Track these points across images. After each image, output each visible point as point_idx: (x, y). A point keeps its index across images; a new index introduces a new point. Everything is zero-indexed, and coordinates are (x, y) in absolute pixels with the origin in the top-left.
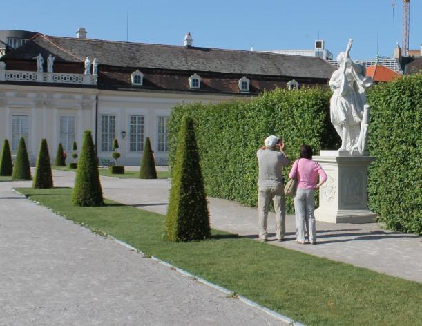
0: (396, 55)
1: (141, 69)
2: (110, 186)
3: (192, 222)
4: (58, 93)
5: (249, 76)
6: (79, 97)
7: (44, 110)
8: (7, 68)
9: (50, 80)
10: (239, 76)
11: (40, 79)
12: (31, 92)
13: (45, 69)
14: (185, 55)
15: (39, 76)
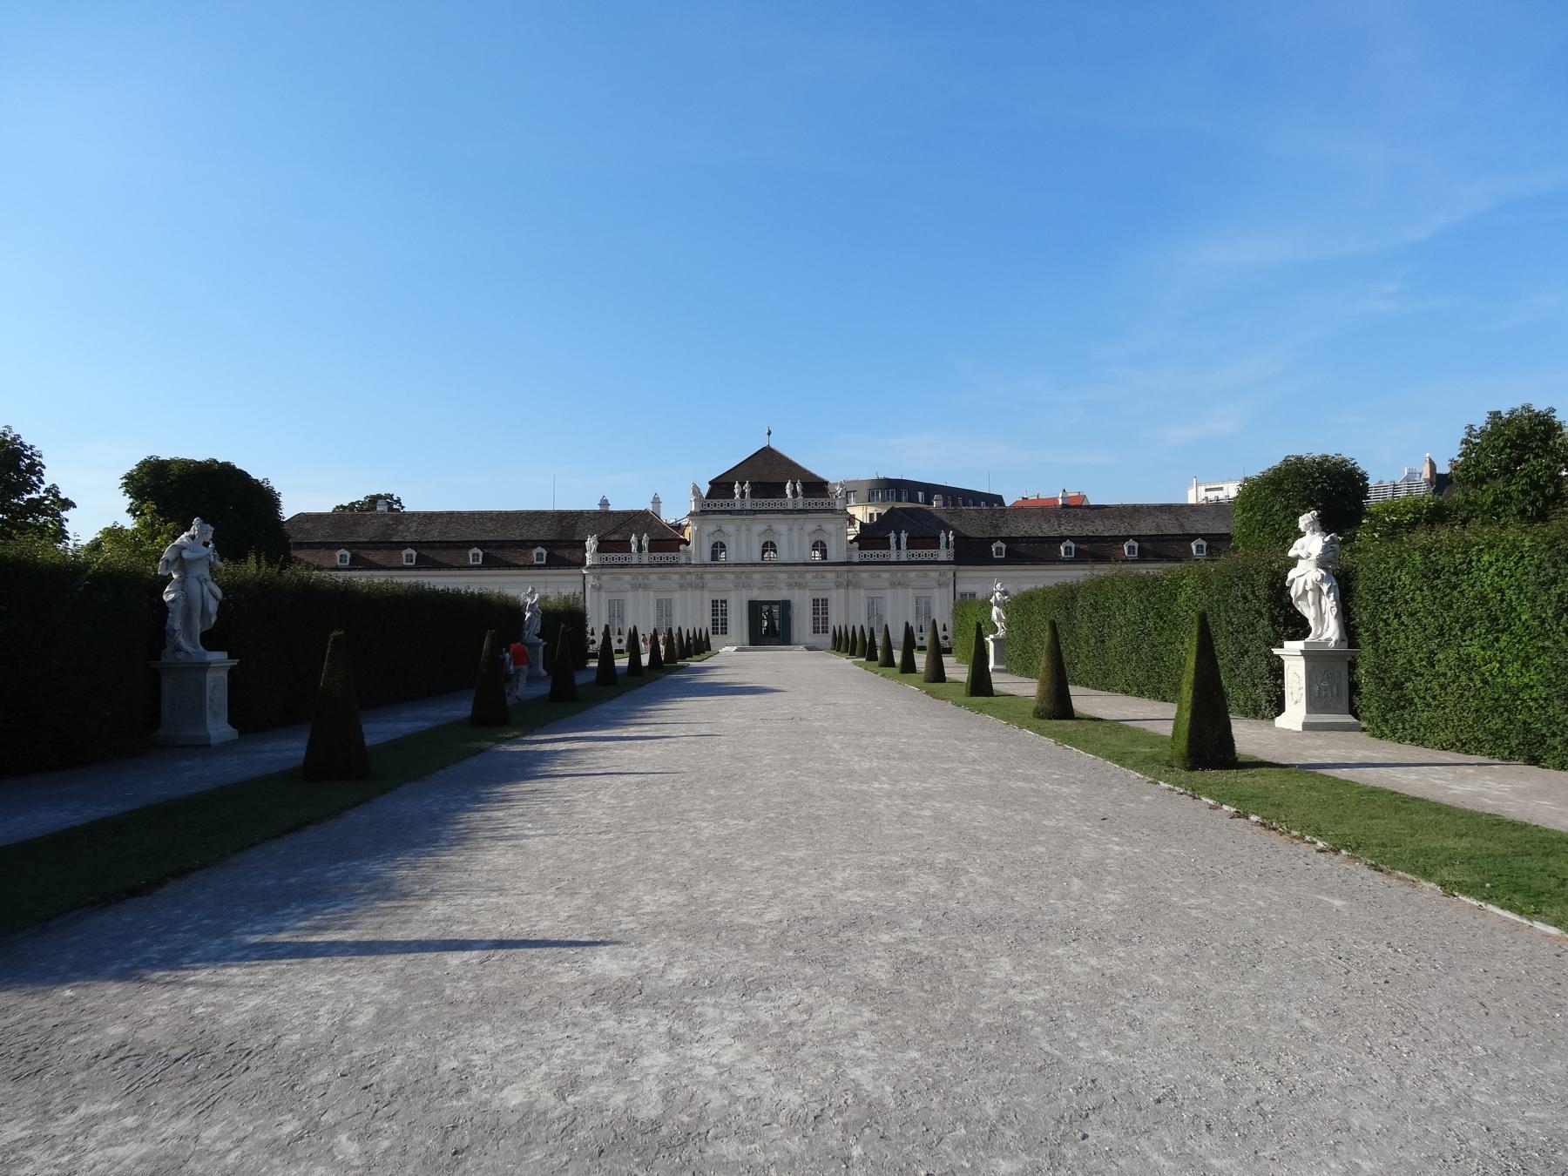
0: (1426, 474)
1: (1003, 540)
2: (1084, 700)
3: (1057, 707)
4: (913, 573)
5: (1136, 538)
6: (934, 575)
7: (900, 590)
8: (860, 548)
9: (904, 558)
10: (1126, 538)
11: (893, 558)
12: (885, 574)
13: (899, 548)
14: (1058, 517)
15: (893, 555)
